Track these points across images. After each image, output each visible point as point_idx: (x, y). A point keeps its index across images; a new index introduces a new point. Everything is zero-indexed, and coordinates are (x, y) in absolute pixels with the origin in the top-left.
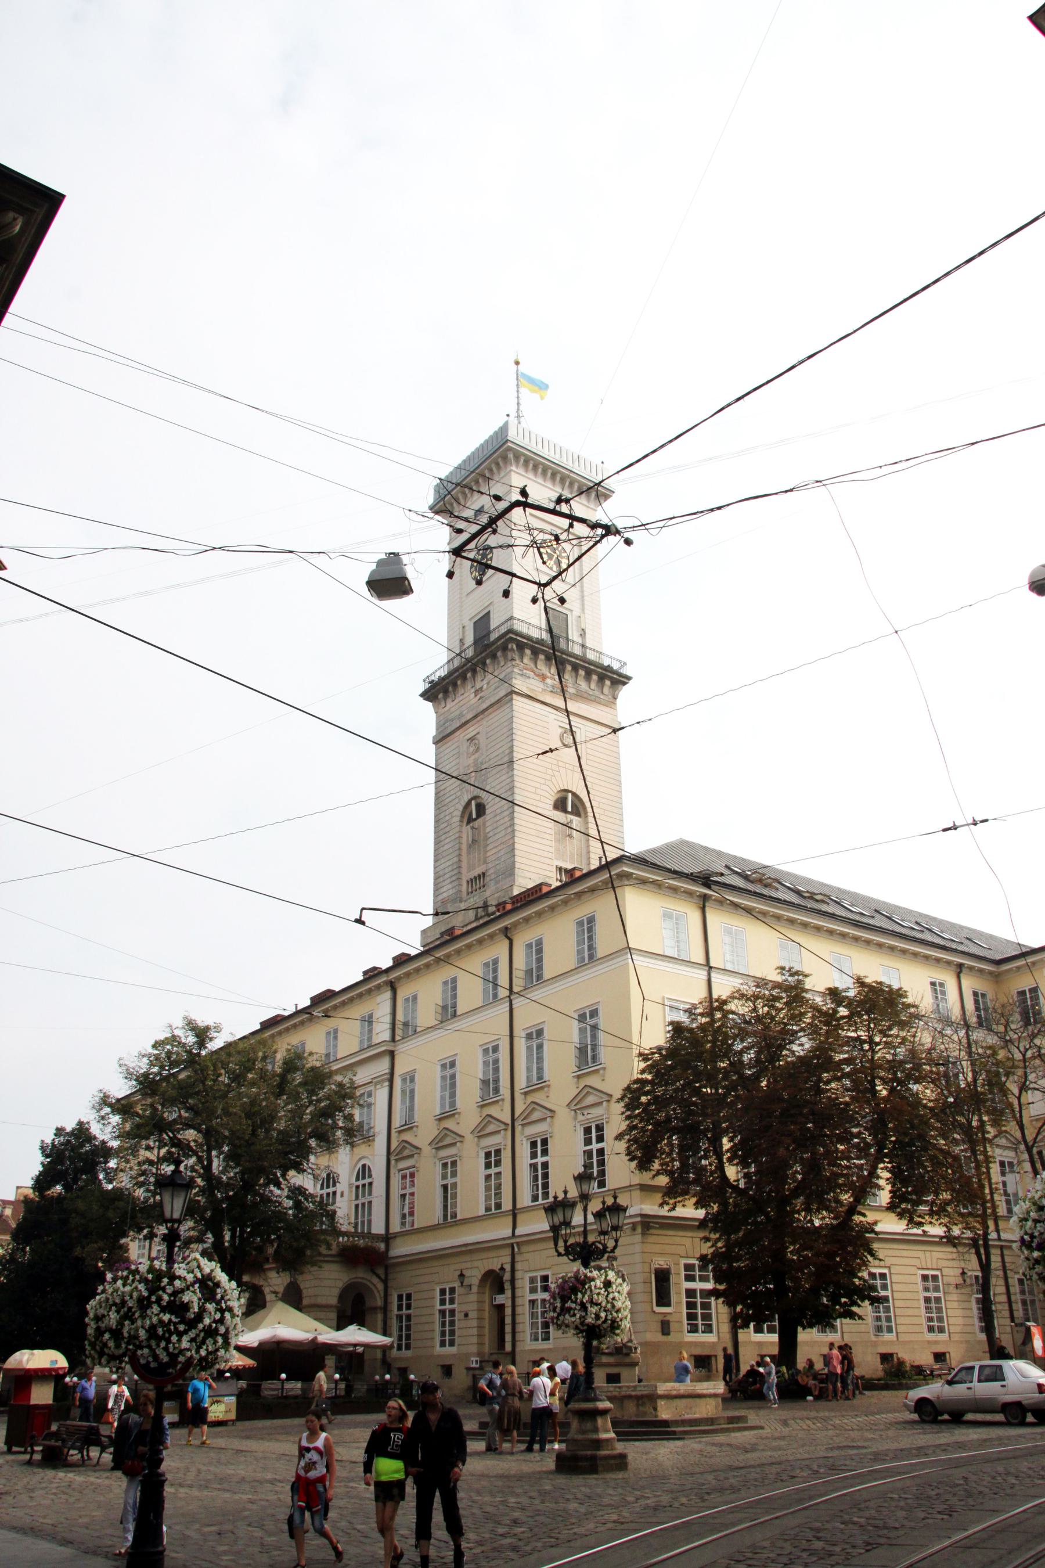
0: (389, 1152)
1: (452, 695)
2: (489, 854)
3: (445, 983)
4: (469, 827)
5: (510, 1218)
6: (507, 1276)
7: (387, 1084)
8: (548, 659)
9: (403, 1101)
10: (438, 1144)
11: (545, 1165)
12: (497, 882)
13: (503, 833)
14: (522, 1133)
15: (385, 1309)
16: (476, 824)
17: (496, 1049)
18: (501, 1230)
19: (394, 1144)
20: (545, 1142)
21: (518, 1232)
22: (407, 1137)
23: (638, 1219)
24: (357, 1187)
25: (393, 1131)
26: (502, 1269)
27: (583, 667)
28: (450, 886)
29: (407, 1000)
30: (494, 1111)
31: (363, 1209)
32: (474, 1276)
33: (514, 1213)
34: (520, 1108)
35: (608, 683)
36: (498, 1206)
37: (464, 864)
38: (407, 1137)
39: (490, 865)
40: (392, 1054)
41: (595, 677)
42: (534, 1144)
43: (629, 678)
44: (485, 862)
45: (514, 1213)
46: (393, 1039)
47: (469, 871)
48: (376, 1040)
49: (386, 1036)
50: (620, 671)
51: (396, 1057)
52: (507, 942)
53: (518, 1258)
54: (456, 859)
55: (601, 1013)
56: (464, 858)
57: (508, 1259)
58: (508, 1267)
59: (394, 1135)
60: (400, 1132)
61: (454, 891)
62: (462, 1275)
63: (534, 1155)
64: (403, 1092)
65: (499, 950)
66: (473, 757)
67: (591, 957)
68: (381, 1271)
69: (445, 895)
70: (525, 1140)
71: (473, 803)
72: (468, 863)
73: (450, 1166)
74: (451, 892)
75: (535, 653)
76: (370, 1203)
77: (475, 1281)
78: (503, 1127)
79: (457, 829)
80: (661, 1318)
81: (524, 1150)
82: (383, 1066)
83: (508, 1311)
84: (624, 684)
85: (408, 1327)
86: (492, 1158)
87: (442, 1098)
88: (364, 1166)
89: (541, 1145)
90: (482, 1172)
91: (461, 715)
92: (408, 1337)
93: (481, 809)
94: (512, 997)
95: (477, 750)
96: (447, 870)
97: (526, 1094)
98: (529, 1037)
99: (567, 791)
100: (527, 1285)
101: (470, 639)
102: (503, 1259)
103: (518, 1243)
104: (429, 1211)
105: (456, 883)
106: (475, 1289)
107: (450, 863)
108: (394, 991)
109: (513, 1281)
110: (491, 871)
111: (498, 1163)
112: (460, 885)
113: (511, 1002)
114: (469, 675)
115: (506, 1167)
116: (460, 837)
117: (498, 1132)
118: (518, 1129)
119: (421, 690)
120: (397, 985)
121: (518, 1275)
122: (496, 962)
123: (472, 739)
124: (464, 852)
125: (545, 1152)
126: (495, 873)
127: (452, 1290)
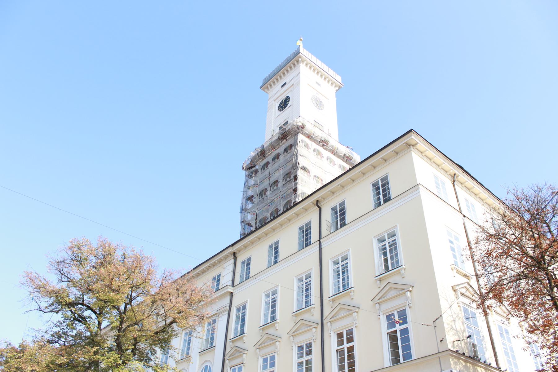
7: (227, 312)
9: (237, 323)
10: (260, 346)
11: (351, 349)
17: (308, 277)
22: (239, 344)
30: (306, 316)
38: (239, 344)
42: (340, 336)
52: (318, 209)
63: (340, 343)
64: (237, 317)
70: (332, 333)
87: (266, 315)
88: (206, 367)
90: (295, 360)
94: (321, 240)
108: (235, 259)
111: (309, 353)
113: (320, 244)
115: (315, 357)
118: (327, 326)
120: (237, 255)
125: (350, 340)
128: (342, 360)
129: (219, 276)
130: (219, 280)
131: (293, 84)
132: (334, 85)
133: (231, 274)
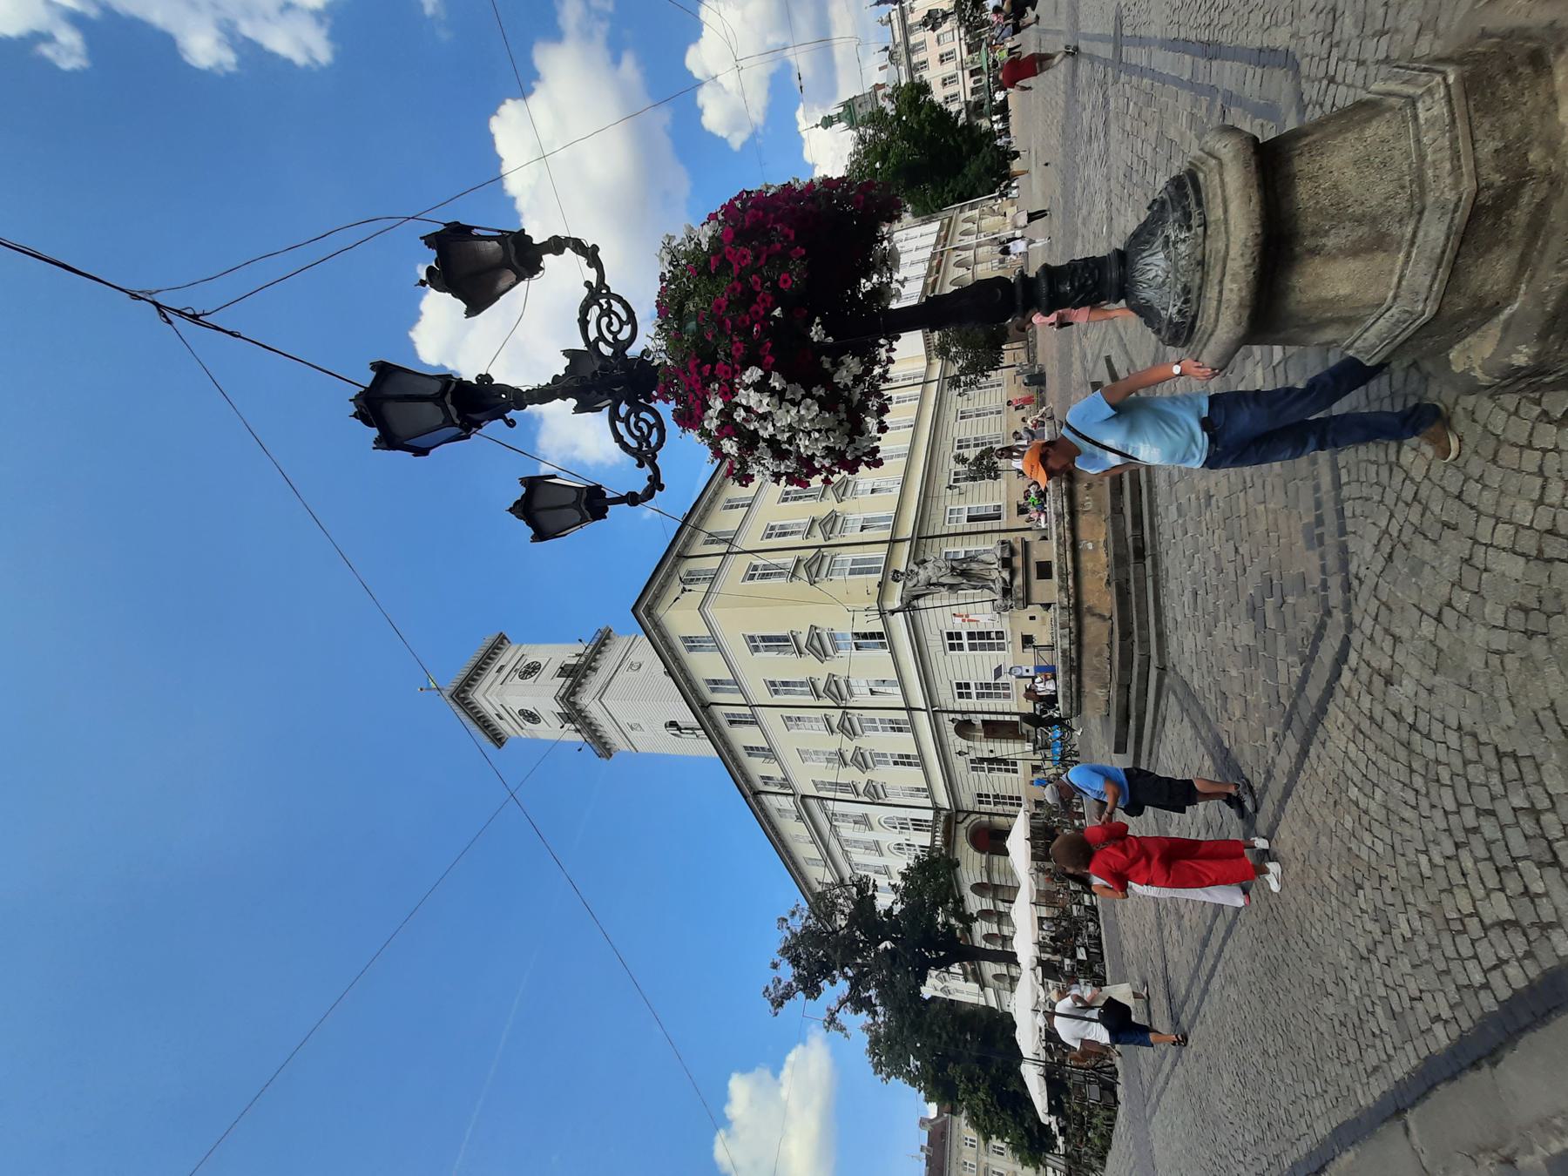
3: (749, 755)
6: (959, 717)
15: (990, 814)
17: (789, 718)
18: (923, 719)
19: (867, 799)
24: (902, 828)
26: (953, 721)
29: (766, 783)
30: (835, 722)
31: (918, 825)
32: (961, 744)
36: (905, 722)
40: (803, 797)
45: (910, 709)
46: (793, 795)
49: (791, 799)
51: (807, 794)
55: (751, 634)
57: (945, 715)
58: (952, 716)
59: (860, 799)
60: (858, 795)
62: (960, 753)
65: (719, 712)
68: (961, 817)
76: (912, 820)
77: (964, 742)
82: (813, 803)
83: (987, 717)
85: (1004, 797)
92: (1011, 798)
97: (818, 696)
98: (776, 692)
100: (965, 700)
102: (945, 720)
104: (914, 776)
106: (970, 744)
109: (963, 713)
121: (957, 708)
127: (972, 761)
133: (779, 797)
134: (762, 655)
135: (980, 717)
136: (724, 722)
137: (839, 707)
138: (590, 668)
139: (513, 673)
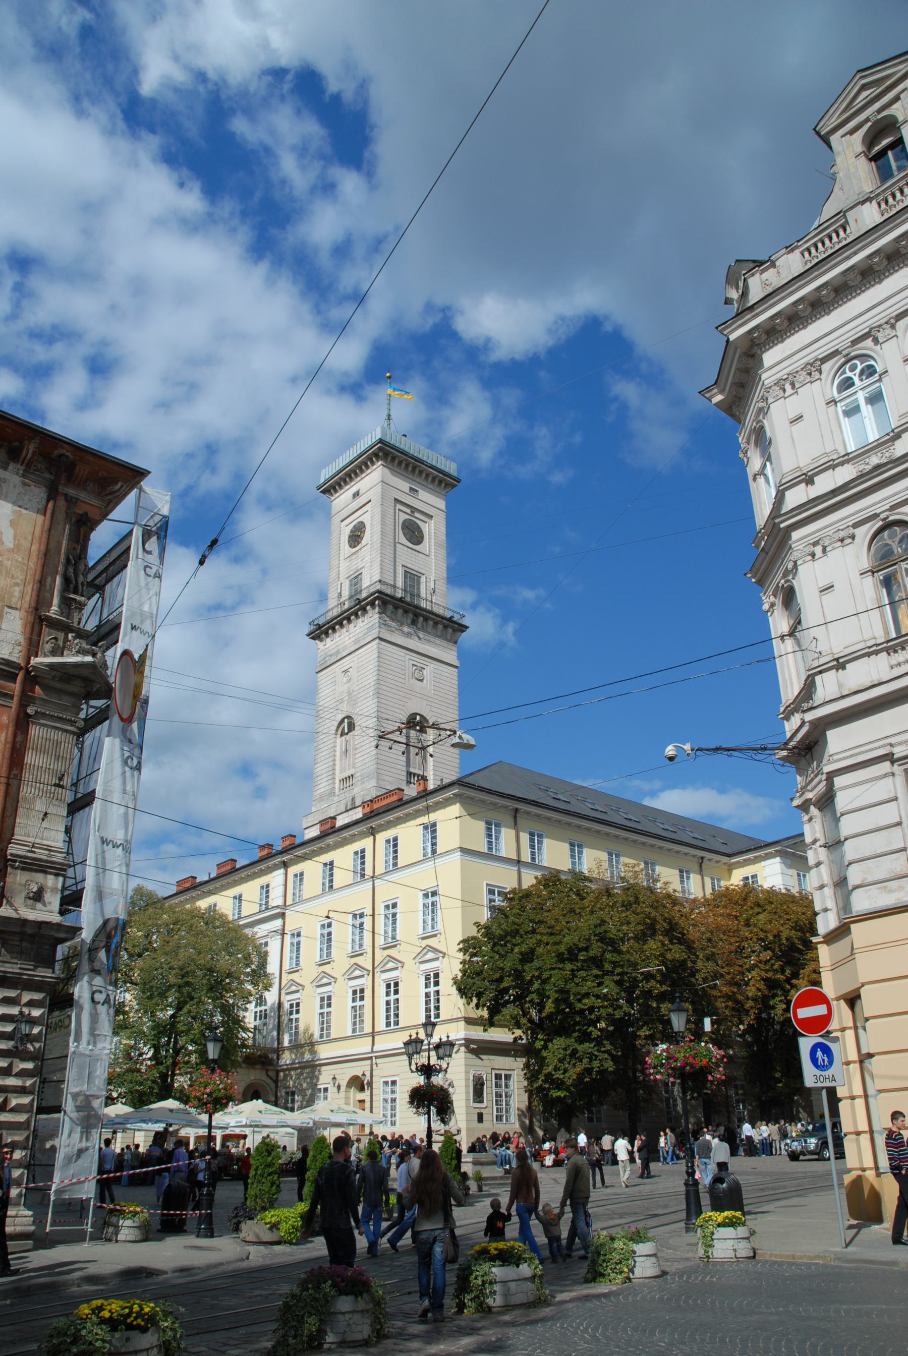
0: (280, 989)
1: (331, 636)
2: (357, 761)
4: (343, 738)
5: (370, 1038)
8: (406, 612)
12: (363, 783)
13: (368, 746)
14: (380, 977)
16: (348, 737)
18: (362, 1046)
20: (396, 984)
21: (376, 1048)
23: (463, 1042)
25: (283, 972)
26: (364, 1075)
27: (432, 619)
28: (327, 783)
29: (296, 876)
33: (373, 1034)
34: (379, 958)
35: (450, 631)
36: (362, 1029)
37: (337, 767)
38: (294, 976)
39: (358, 770)
40: (283, 915)
41: (440, 627)
42: (388, 986)
43: (467, 627)
44: (354, 767)
45: (373, 1034)
47: (341, 773)
48: (272, 903)
49: (280, 902)
50: (460, 622)
53: (374, 1066)
54: (331, 763)
56: (338, 762)
57: (369, 1068)
58: (368, 1074)
61: (330, 787)
62: (334, 1078)
63: (388, 994)
65: (366, 843)
66: (346, 686)
67: (434, 852)
69: (322, 790)
71: (346, 720)
72: (341, 766)
73: (326, 1001)
74: (327, 788)
75: (396, 608)
77: (344, 1084)
78: (366, 972)
79: (333, 741)
80: (478, 1111)
81: (381, 989)
82: (278, 923)
84: (463, 631)
86: (358, 994)
89: (393, 987)
91: (338, 652)
93: (351, 727)
95: (349, 681)
96: (324, 771)
98: (387, 907)
99: (416, 714)
101: (346, 594)
103: (376, 1057)
105: (330, 782)
107: (327, 765)
110: (358, 774)
111: (362, 998)
112: (334, 783)
114: (345, 622)
115: (367, 1002)
116: (335, 746)
117: (363, 976)
119: (307, 632)
122: (363, 851)
123: (345, 671)
124: (338, 758)
125: (396, 992)
126: (361, 775)
128: (388, 1010)
129: (268, 886)
130: (267, 892)
131: (370, 501)
132: (443, 485)
134: (421, 901)
135: (368, 1099)
136: (357, 846)
137: (374, 968)
138: (416, 616)
139: (408, 511)
